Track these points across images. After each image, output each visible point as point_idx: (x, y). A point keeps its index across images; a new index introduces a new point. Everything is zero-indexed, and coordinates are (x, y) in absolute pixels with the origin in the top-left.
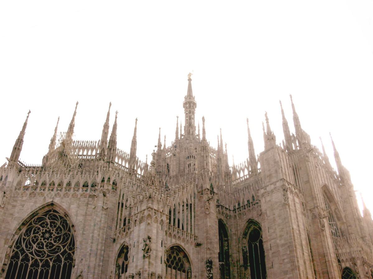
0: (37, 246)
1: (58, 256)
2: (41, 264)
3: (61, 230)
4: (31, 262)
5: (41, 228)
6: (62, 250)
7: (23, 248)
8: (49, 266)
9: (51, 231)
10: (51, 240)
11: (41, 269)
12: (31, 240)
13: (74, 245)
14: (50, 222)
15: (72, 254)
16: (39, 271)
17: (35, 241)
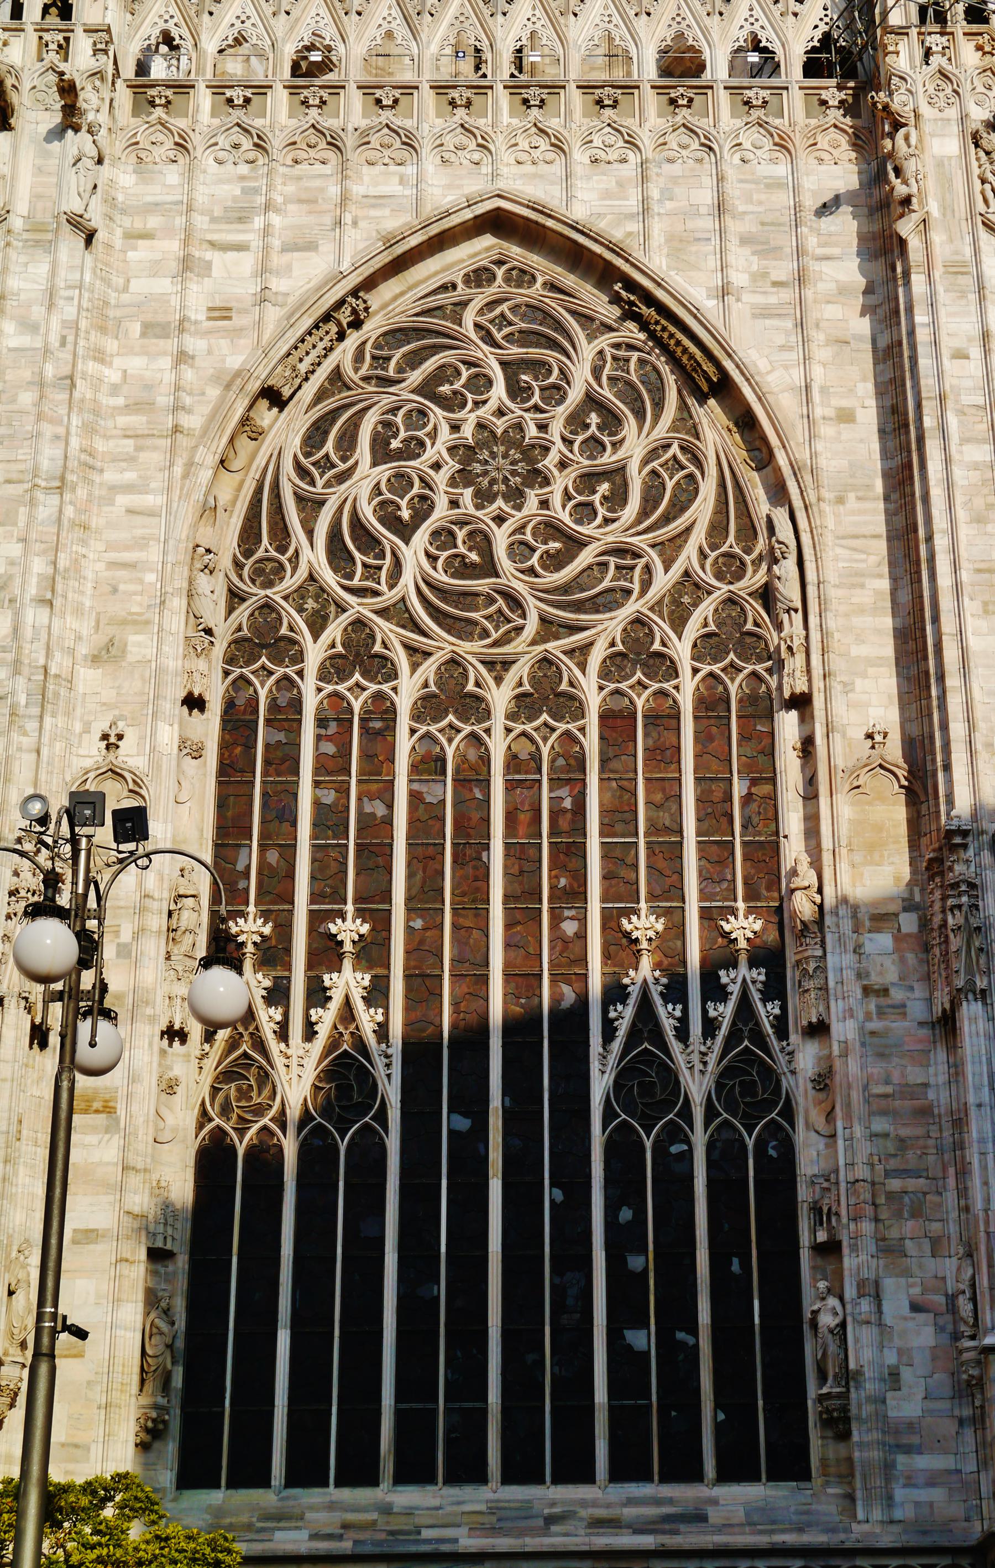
0: (432, 558)
1: (638, 621)
2: (500, 698)
3: (612, 421)
4: (407, 690)
5: (437, 414)
6: (663, 581)
7: (311, 578)
8: (570, 705)
9: (532, 431)
10: (544, 504)
11: (508, 730)
12: (368, 512)
13: (748, 532)
14: (504, 364)
15: (755, 608)
16: (498, 747)
17: (405, 514)
